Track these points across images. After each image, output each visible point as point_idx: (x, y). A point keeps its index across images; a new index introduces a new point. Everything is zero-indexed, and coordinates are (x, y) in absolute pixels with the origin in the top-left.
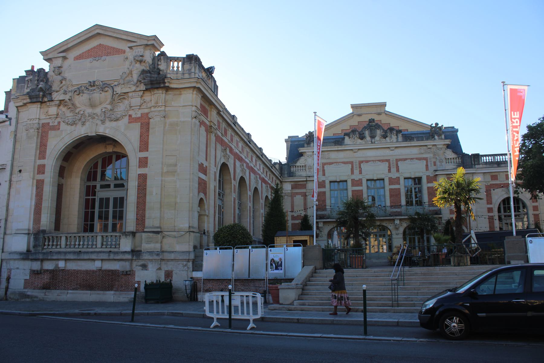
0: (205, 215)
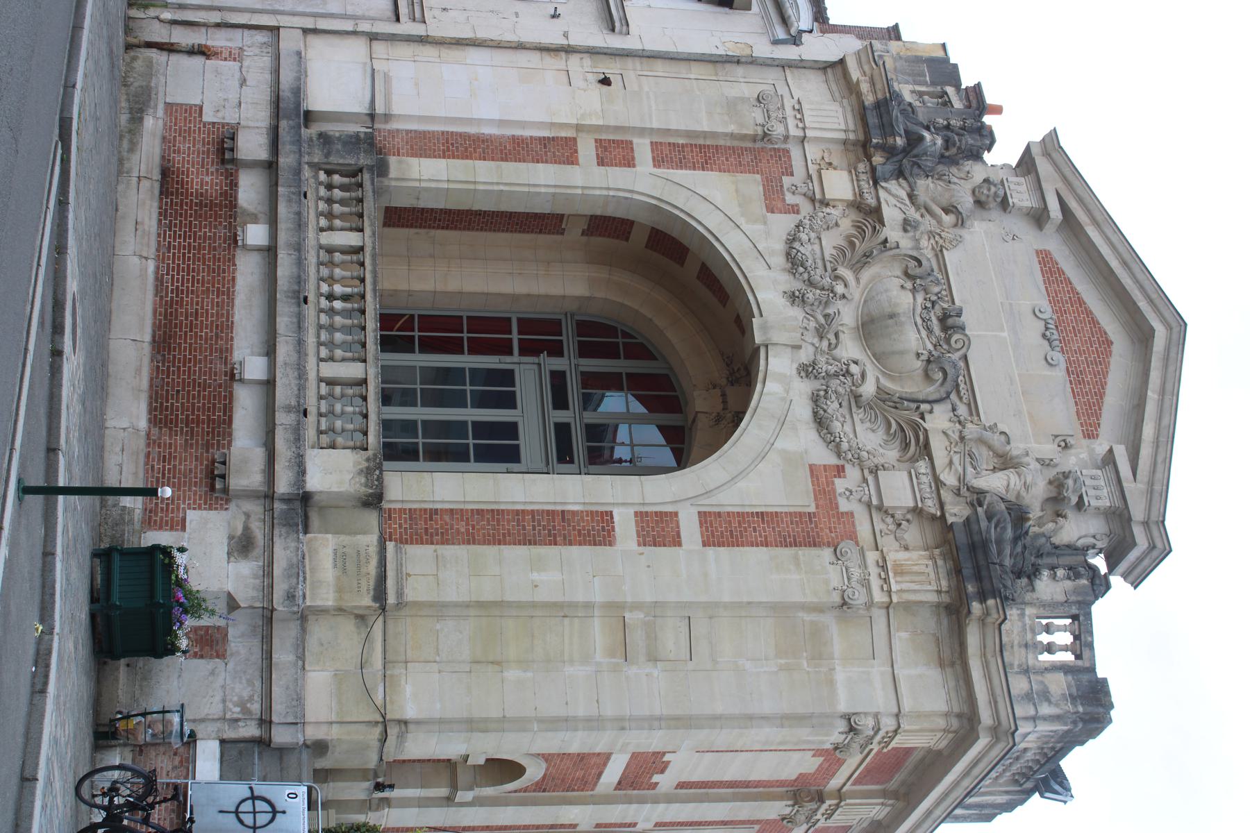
0: (454, 787)
